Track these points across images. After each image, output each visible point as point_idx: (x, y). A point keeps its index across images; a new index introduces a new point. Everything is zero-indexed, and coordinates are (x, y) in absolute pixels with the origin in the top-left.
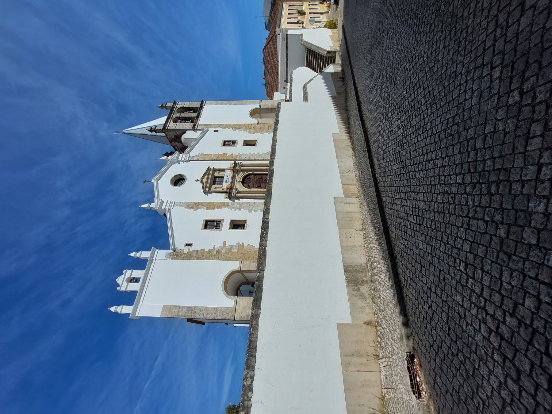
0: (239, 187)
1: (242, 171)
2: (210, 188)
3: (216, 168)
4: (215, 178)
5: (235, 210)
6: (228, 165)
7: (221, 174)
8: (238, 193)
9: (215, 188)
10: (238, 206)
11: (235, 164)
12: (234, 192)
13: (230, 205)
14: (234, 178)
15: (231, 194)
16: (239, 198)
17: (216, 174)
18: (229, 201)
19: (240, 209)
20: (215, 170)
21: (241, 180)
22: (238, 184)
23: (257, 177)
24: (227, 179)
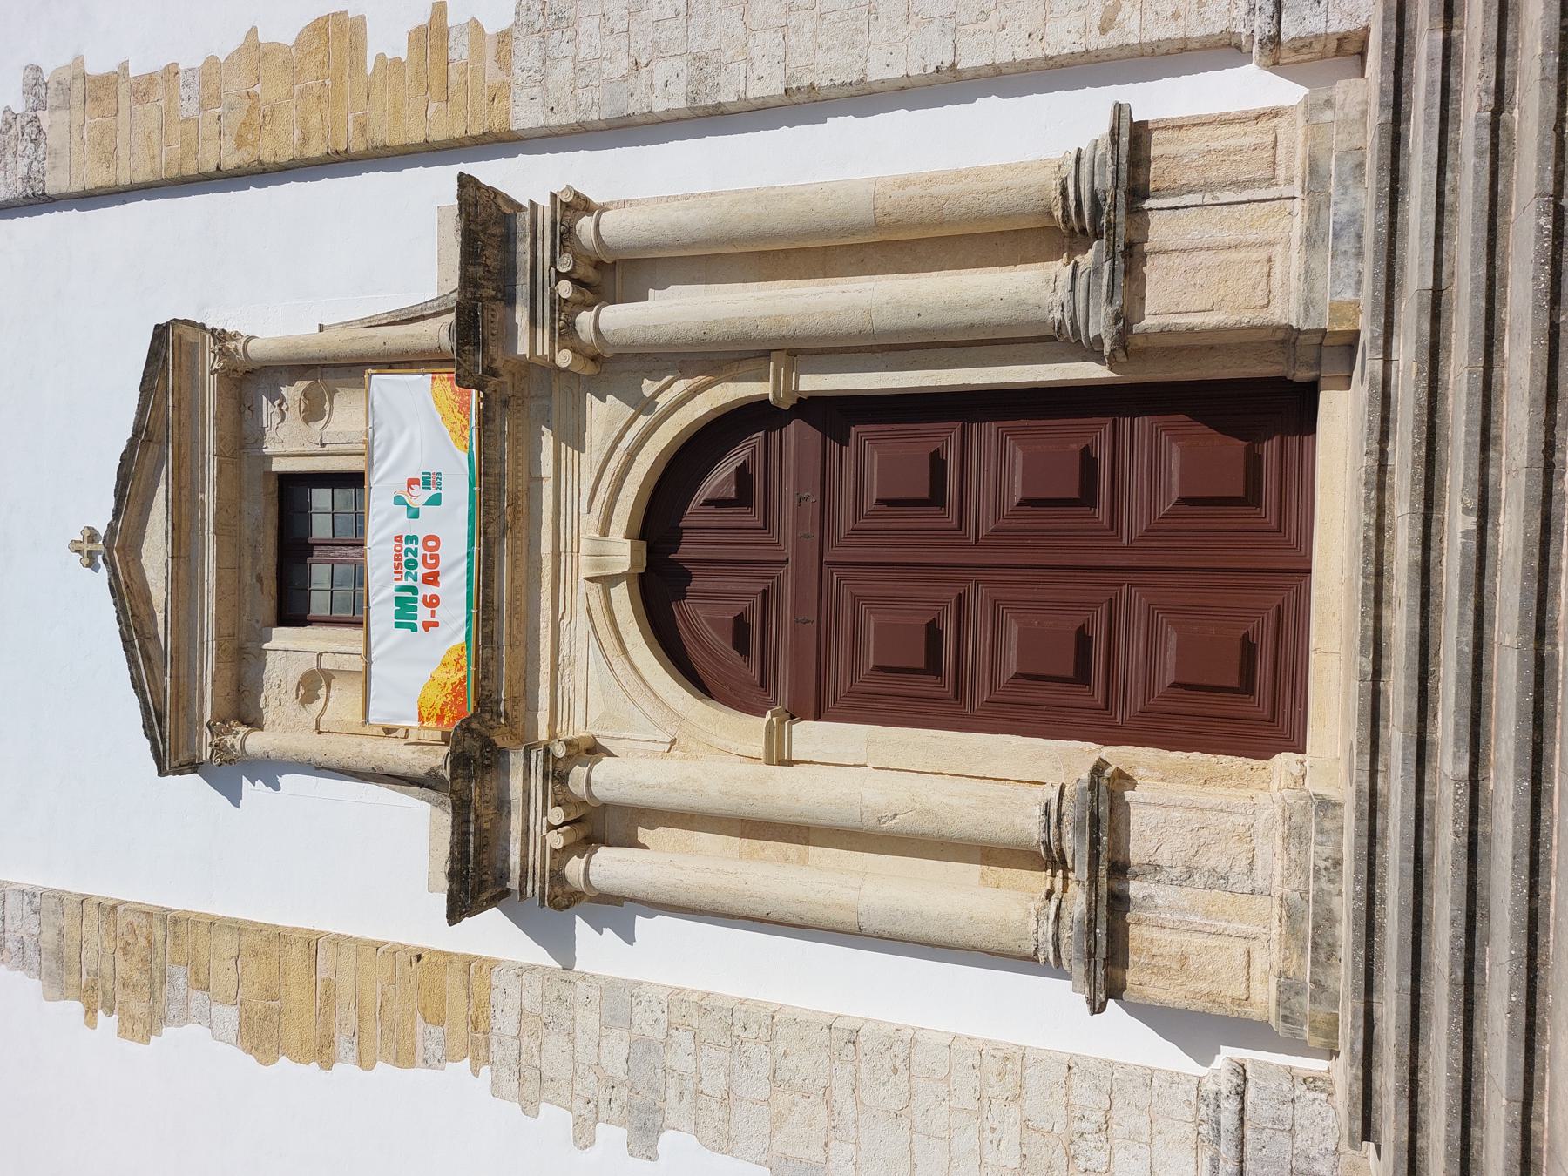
0: (616, 701)
1: (617, 367)
2: (243, 708)
3: (271, 323)
4: (293, 490)
5: (583, 1137)
6: (381, 252)
7: (346, 414)
8: (597, 825)
9: (313, 684)
10: (615, 1057)
11: (485, 226)
12: (531, 828)
13: (505, 1024)
14: (503, 509)
15: (505, 814)
16: (618, 909)
17: (289, 442)
18: (492, 934)
19: (645, 1133)
20: (252, 379)
21: (621, 554)
22: (576, 631)
23: (875, 463)
24: (418, 559)
